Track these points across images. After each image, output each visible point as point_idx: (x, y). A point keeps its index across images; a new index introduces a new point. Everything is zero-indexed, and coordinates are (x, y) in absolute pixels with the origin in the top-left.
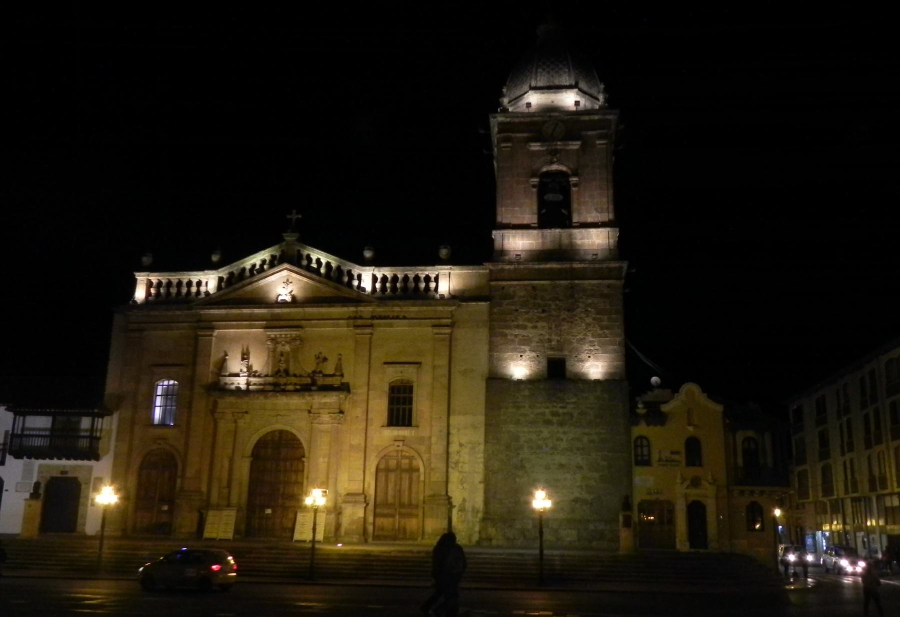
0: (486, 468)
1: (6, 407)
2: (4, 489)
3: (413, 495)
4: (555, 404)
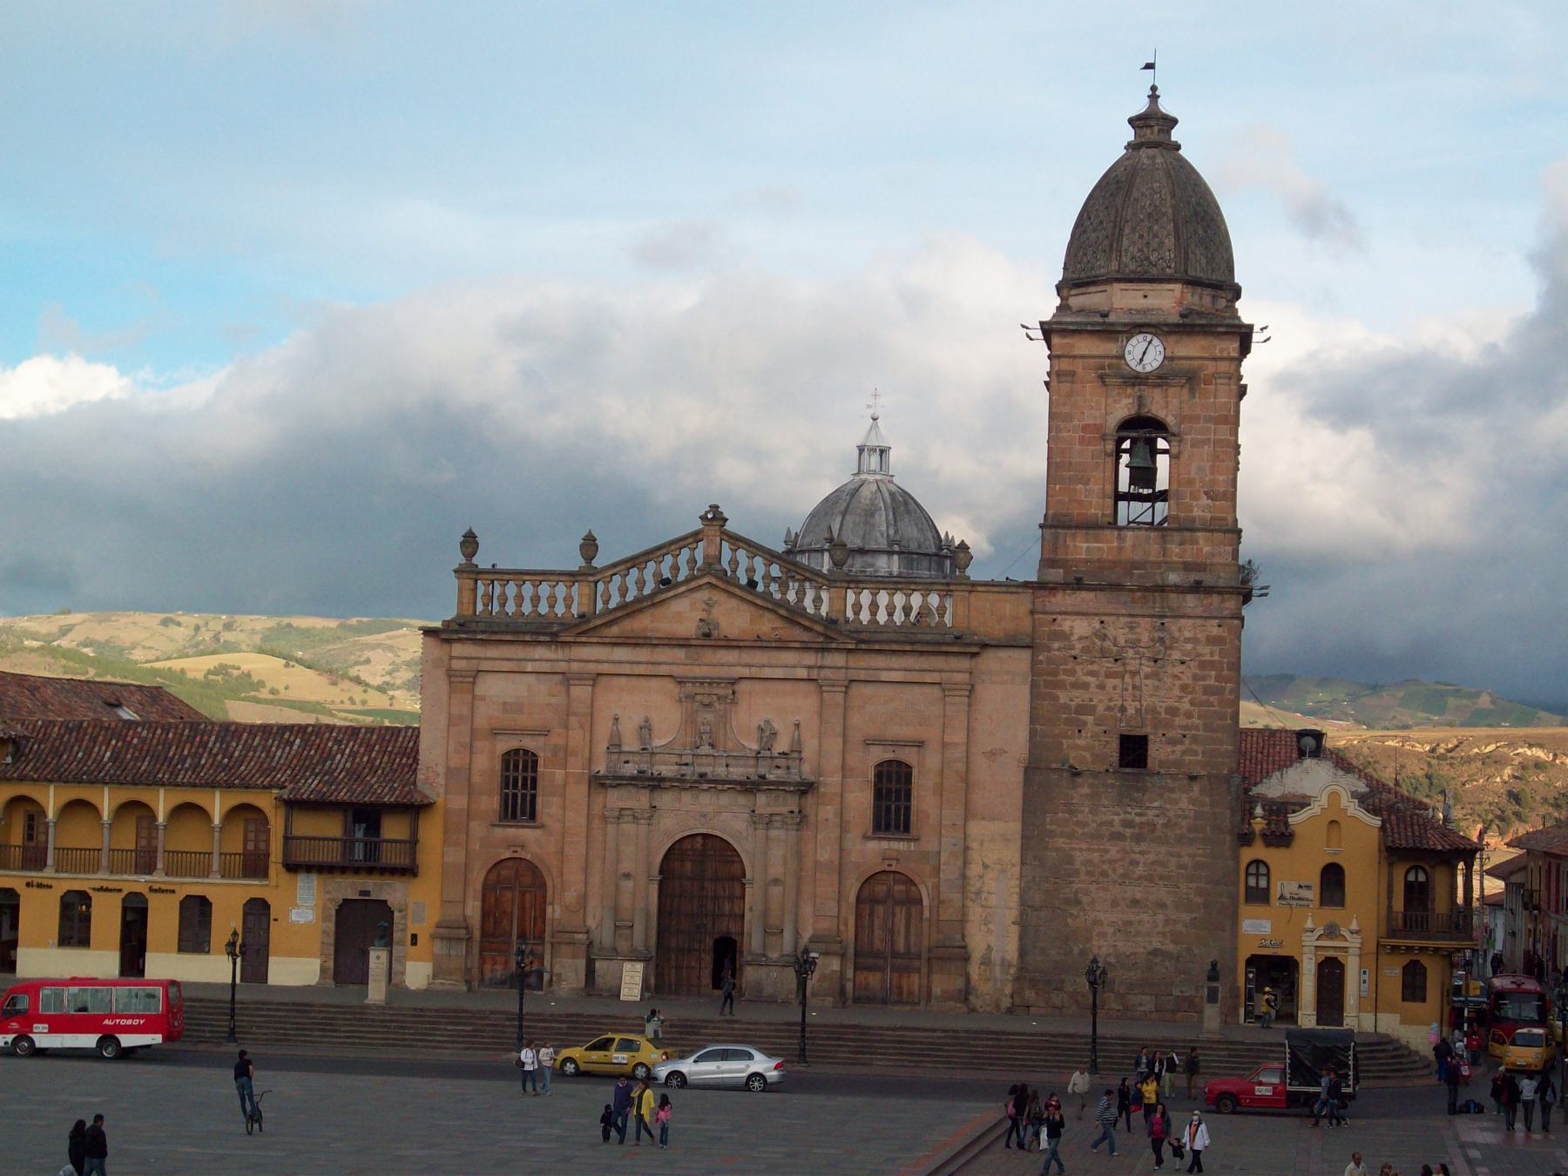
0: (1023, 903)
1: (779, 1060)
2: (272, 918)
3: (913, 939)
4: (1129, 809)
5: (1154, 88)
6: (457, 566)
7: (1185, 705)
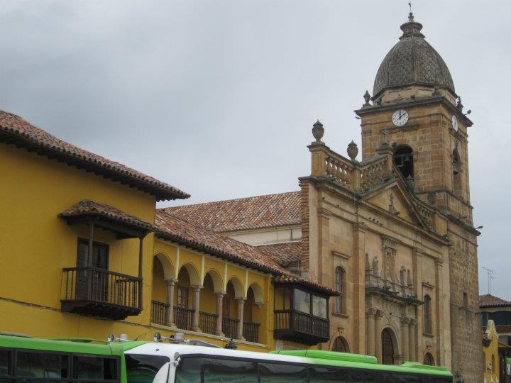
5: (411, 14)
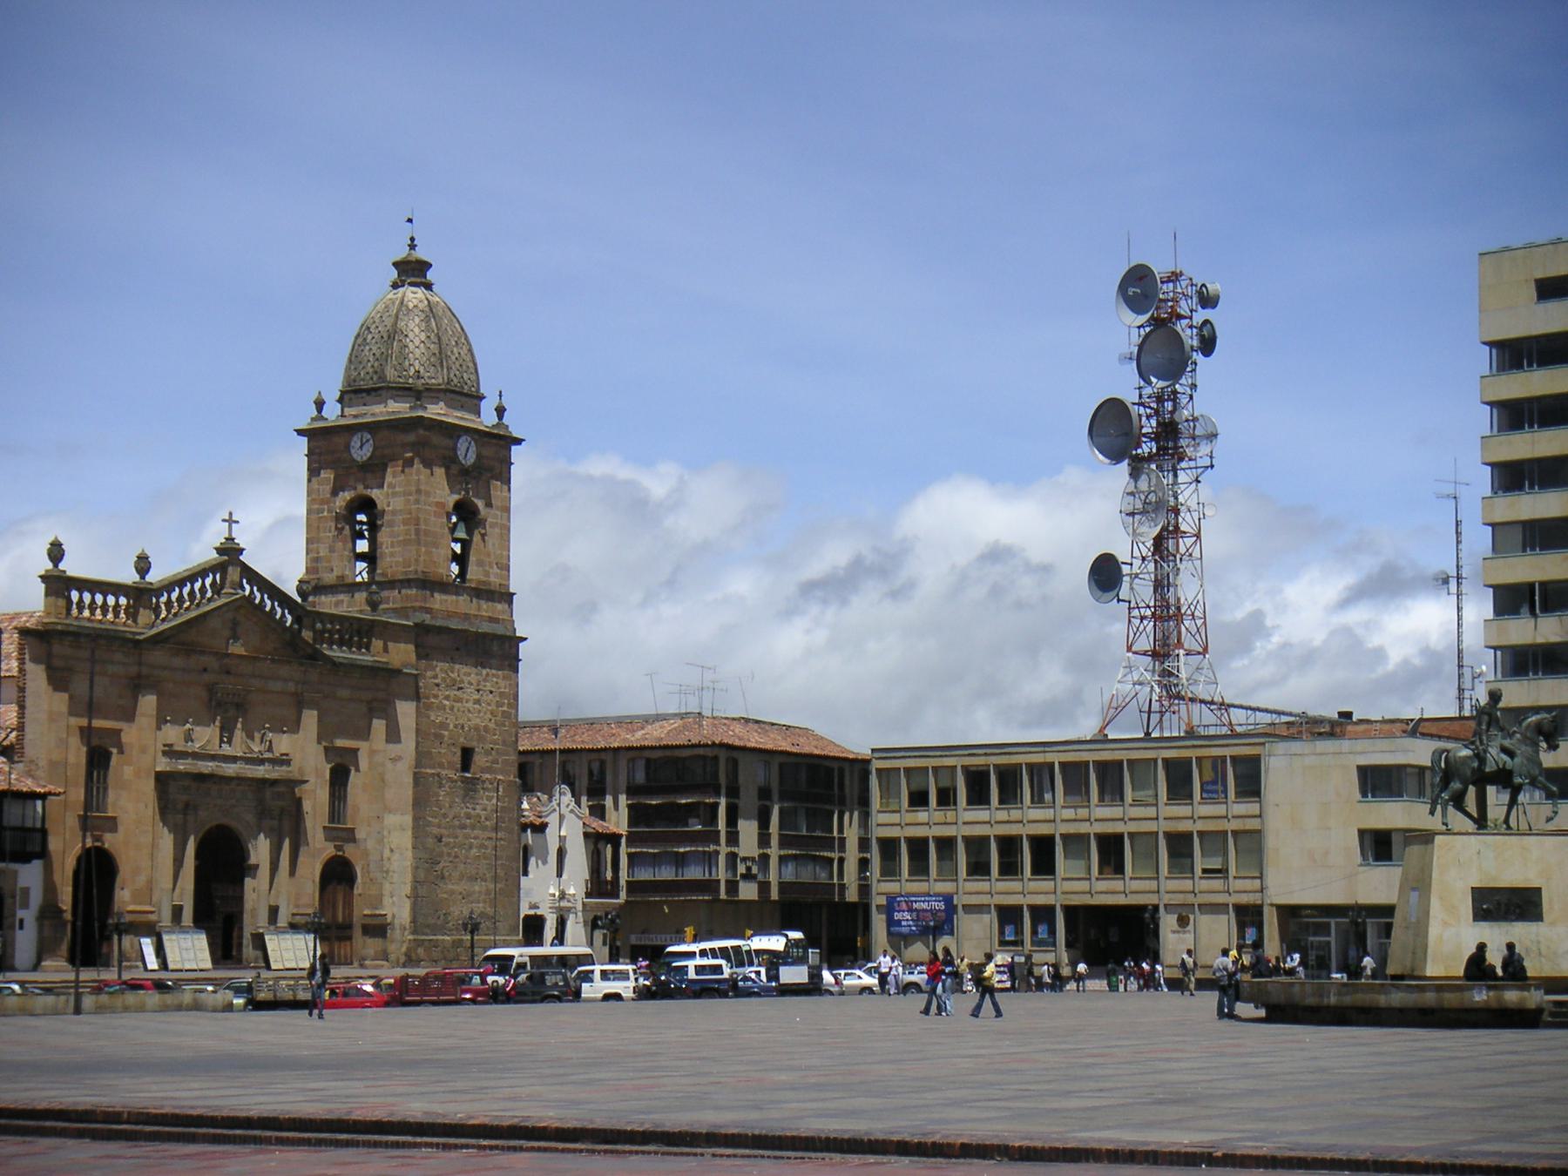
5: (412, 239)
6: (43, 573)
7: (492, 725)
